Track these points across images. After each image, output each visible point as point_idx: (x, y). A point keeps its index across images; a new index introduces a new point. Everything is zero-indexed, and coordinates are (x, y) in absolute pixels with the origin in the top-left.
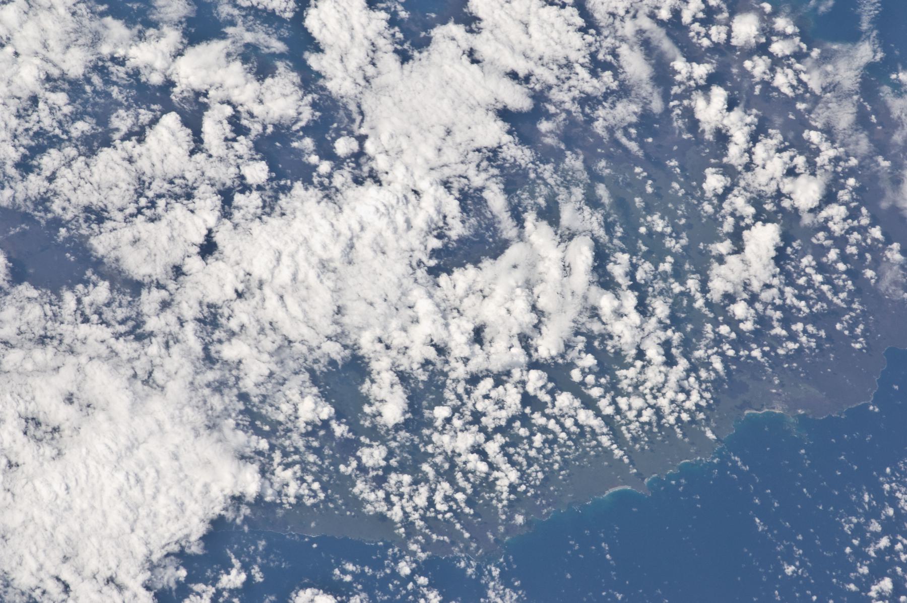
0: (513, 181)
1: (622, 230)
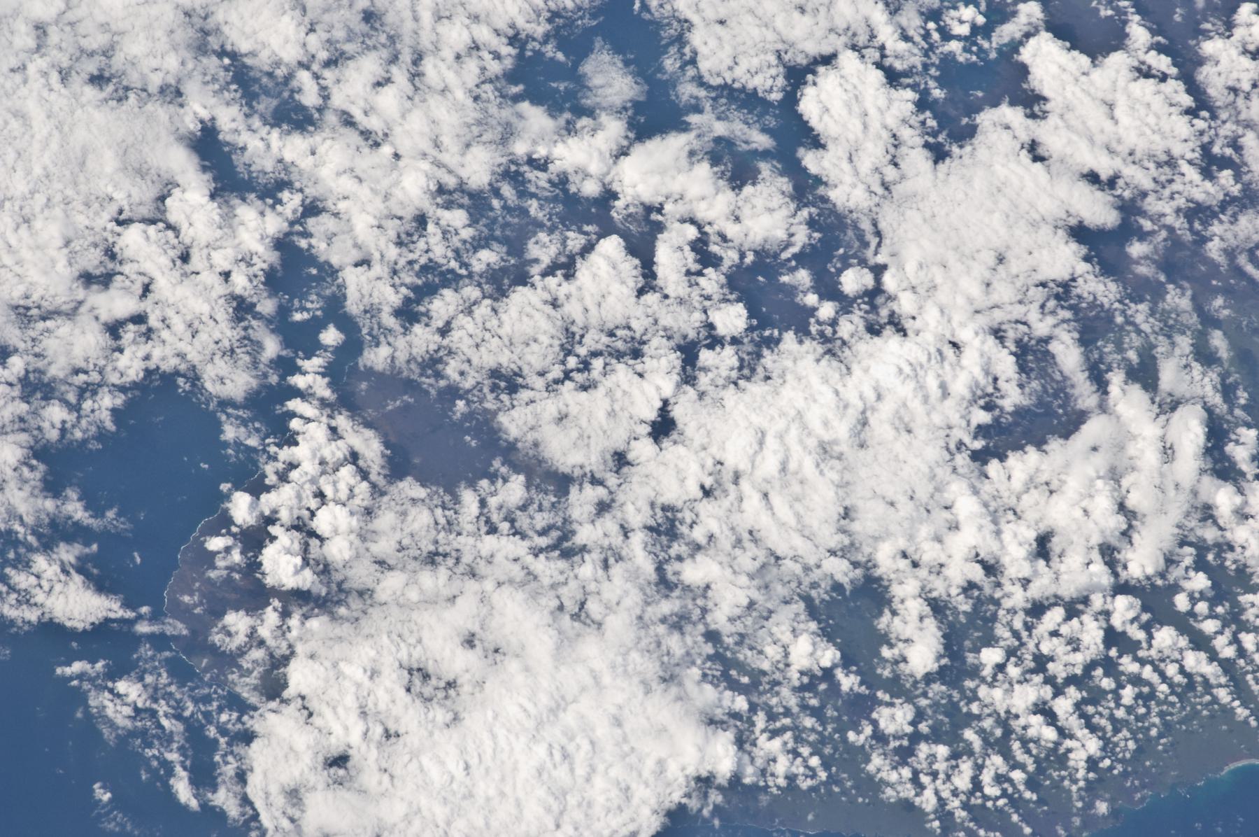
0: (1093, 327)
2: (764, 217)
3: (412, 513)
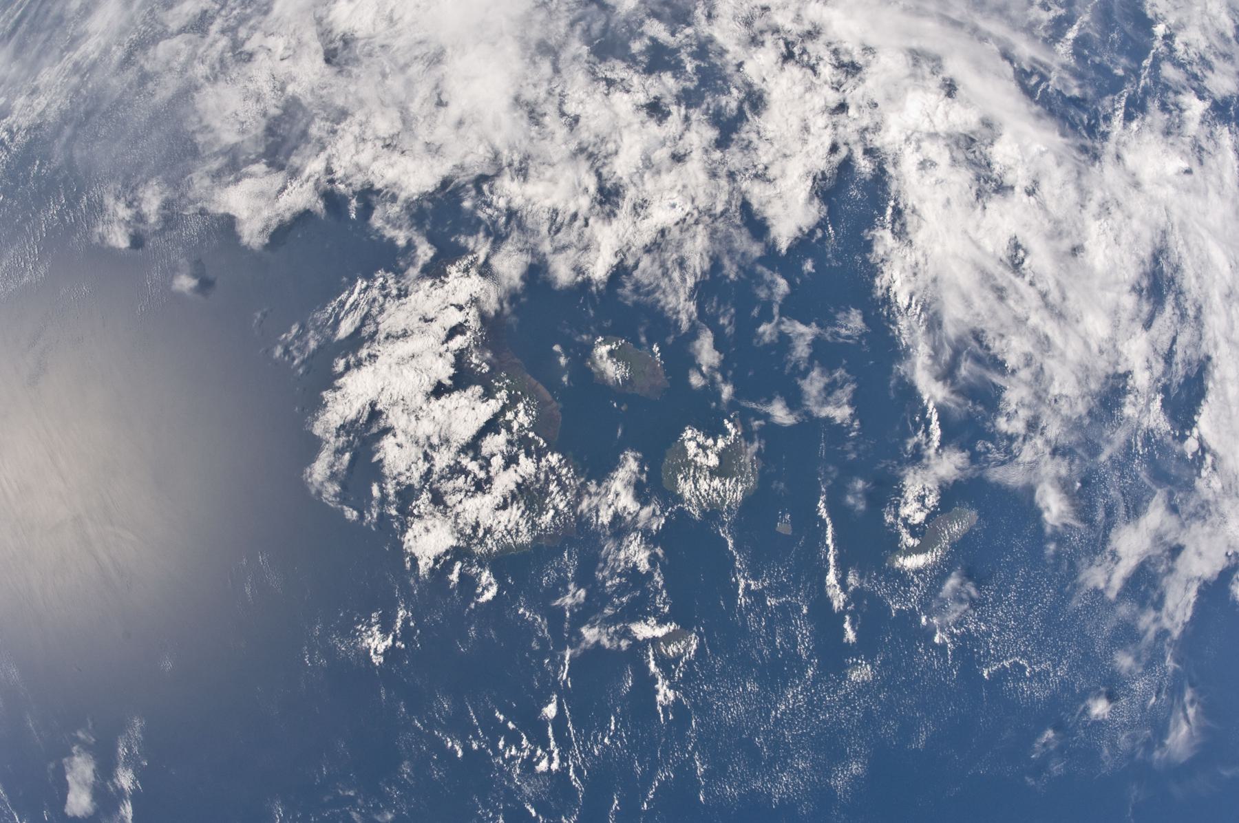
0: (514, 497)
1: (529, 507)
2: (482, 475)
3: (431, 508)
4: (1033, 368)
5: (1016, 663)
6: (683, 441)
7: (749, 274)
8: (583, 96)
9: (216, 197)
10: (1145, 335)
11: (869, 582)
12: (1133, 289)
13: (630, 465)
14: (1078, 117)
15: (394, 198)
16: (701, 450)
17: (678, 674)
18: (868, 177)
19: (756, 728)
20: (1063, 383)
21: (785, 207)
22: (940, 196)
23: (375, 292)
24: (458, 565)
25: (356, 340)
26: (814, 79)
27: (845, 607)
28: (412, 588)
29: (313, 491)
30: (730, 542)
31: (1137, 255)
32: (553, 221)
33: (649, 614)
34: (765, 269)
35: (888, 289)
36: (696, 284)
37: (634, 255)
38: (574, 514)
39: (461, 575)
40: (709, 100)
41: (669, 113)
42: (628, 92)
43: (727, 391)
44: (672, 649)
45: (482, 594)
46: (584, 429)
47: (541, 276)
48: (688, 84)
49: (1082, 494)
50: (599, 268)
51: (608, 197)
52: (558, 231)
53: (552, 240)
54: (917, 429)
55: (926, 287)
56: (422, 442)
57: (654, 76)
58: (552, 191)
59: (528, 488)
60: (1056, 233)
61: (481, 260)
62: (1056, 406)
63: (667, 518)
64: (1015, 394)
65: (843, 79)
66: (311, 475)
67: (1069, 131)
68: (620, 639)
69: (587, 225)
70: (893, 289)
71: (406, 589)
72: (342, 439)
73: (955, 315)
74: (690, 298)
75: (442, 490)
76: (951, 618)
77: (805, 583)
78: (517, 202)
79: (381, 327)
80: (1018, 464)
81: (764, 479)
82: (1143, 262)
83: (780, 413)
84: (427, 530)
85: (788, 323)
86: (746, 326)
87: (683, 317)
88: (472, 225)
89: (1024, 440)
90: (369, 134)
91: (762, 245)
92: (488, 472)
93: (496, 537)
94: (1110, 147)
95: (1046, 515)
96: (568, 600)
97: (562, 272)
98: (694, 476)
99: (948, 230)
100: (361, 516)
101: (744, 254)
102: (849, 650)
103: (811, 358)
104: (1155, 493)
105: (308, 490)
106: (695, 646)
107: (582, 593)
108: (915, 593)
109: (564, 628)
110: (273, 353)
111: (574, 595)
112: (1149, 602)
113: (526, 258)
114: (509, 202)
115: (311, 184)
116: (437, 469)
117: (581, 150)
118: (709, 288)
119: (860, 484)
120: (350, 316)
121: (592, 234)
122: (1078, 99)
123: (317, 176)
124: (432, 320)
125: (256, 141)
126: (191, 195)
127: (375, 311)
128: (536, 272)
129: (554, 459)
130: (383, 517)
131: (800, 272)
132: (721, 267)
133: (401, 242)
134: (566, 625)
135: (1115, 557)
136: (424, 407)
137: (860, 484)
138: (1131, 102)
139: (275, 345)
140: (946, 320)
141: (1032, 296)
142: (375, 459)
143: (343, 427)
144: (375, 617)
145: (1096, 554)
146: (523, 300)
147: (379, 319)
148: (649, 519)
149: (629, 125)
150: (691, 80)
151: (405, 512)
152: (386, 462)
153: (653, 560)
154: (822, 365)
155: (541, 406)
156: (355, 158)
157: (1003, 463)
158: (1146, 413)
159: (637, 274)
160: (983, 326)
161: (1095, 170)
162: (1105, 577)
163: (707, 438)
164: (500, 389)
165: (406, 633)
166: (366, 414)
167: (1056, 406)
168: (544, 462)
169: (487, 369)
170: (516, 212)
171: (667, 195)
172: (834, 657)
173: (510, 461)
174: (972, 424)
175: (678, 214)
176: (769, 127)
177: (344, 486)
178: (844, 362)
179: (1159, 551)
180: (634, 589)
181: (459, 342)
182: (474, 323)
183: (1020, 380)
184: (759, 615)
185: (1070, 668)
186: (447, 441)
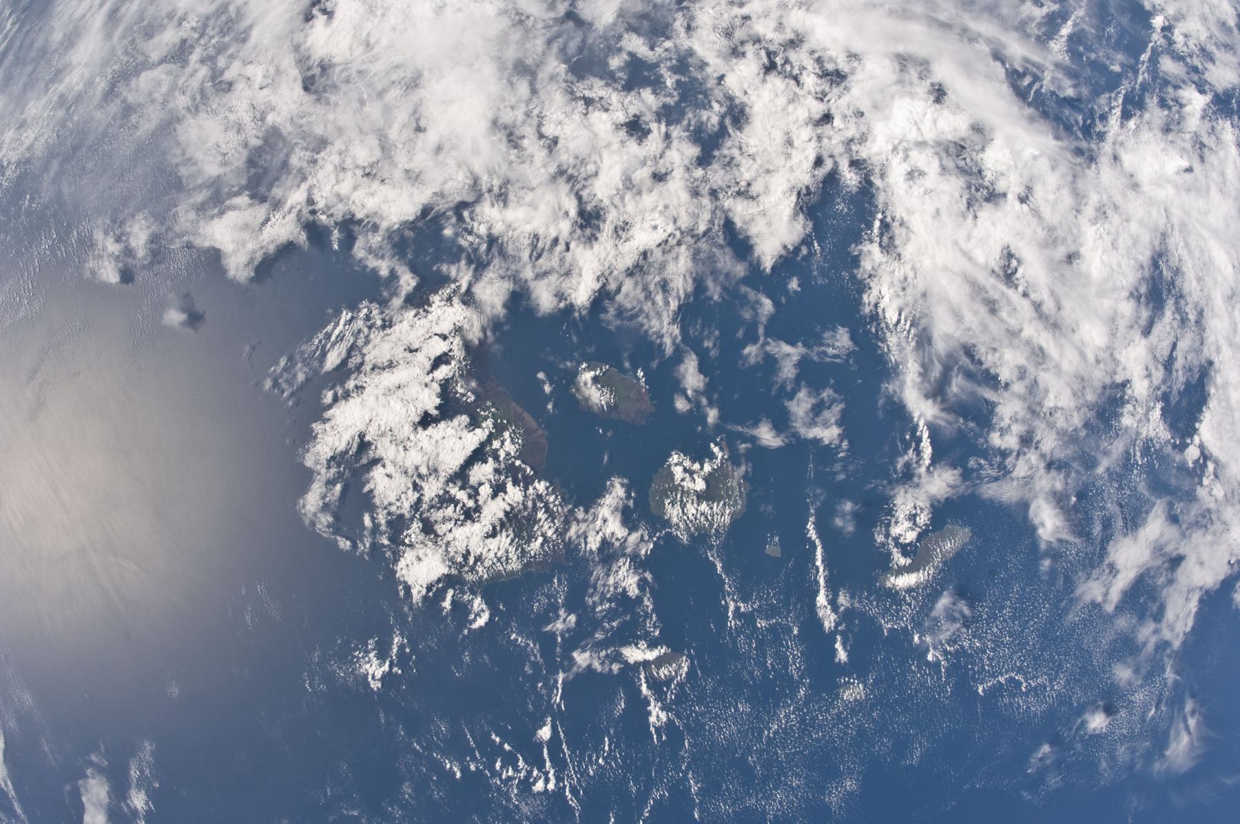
0: (503, 525)
1: (518, 535)
2: (471, 504)
3: (422, 537)
4: (1027, 381)
5: (1011, 678)
6: (670, 466)
7: (732, 294)
8: (562, 117)
9: (201, 231)
10: (1144, 342)
11: (860, 602)
12: (1131, 295)
13: (617, 492)
14: (1072, 117)
15: (375, 228)
16: (687, 475)
17: (670, 697)
18: (854, 190)
19: (749, 747)
20: (1058, 394)
21: (769, 224)
22: (930, 207)
23: (360, 324)
24: (450, 593)
25: (344, 371)
26: (797, 90)
27: (836, 627)
28: (407, 616)
29: (307, 522)
30: (719, 566)
31: (1136, 259)
32: (534, 246)
33: (640, 638)
34: (749, 290)
35: (876, 305)
36: (680, 307)
37: (616, 279)
38: (563, 540)
39: (453, 602)
40: (690, 115)
41: (649, 131)
42: (607, 110)
43: (712, 415)
44: (664, 672)
45: (475, 620)
46: (570, 456)
47: (524, 303)
48: (668, 100)
49: (1079, 507)
50: (582, 293)
51: (589, 220)
52: (539, 256)
53: (534, 266)
54: (907, 446)
55: (916, 301)
56: (410, 472)
57: (633, 93)
58: (532, 216)
59: (516, 516)
60: (1051, 240)
61: (464, 289)
62: (1051, 419)
63: (655, 543)
64: (1009, 408)
65: (827, 89)
66: (304, 506)
67: (1063, 133)
68: (611, 663)
69: (568, 249)
70: (882, 305)
71: (401, 617)
72: (333, 470)
73: (945, 331)
74: (674, 321)
75: (432, 520)
76: (944, 637)
77: (795, 604)
78: (498, 229)
79: (367, 358)
80: (1012, 479)
81: (752, 502)
82: (1142, 267)
83: (767, 436)
84: (419, 559)
85: (773, 344)
86: (731, 348)
87: (667, 341)
88: (454, 253)
89: (1018, 455)
90: (349, 163)
91: (746, 264)
92: (476, 501)
93: (486, 565)
94: (1107, 147)
95: (1040, 531)
96: (559, 626)
97: (545, 299)
98: (681, 501)
99: (938, 242)
100: (355, 546)
101: (727, 275)
102: (842, 670)
103: (797, 380)
104: (1153, 505)
105: (301, 520)
106: (686, 669)
107: (572, 618)
108: (907, 611)
109: (556, 653)
110: (263, 386)
111: (565, 620)
112: (1148, 613)
113: (508, 286)
114: (490, 228)
115: (293, 215)
116: (426, 499)
117: (561, 172)
118: (693, 310)
119: (848, 506)
120: (336, 347)
121: (574, 259)
122: (1072, 99)
123: (299, 207)
124: (416, 350)
125: (238, 172)
126: (177, 228)
127: (360, 342)
128: (519, 299)
129: (541, 486)
130: (375, 546)
131: (785, 291)
132: (706, 289)
133: (384, 272)
134: (558, 650)
135: (1113, 570)
136: (412, 437)
137: (848, 506)
138: (1128, 99)
139: (265, 378)
140: (936, 336)
141: (1025, 307)
142: (366, 489)
143: (333, 458)
144: (371, 643)
145: (1093, 567)
146: (506, 328)
147: (365, 351)
148: (637, 545)
149: (608, 145)
150: (671, 95)
151: (397, 541)
152: (376, 493)
153: (642, 584)
154: (809, 385)
155: (527, 434)
156: (336, 188)
157: (996, 479)
158: (1145, 422)
159: (619, 298)
160: (974, 341)
161: (1091, 173)
162: (1103, 590)
163: (694, 462)
164: (486, 418)
165: (402, 659)
166: (355, 446)
167: (1051, 419)
168: (531, 491)
169: (473, 398)
170: (497, 238)
171: (648, 216)
172: (826, 676)
173: (499, 489)
174: (965, 440)
175: (660, 236)
176: (752, 142)
177: (336, 517)
178: (832, 381)
179: (1159, 562)
180: (624, 613)
181: (444, 372)
182: (458, 353)
183: (1013, 393)
184: (748, 637)
185: (1068, 682)
186: (436, 470)
